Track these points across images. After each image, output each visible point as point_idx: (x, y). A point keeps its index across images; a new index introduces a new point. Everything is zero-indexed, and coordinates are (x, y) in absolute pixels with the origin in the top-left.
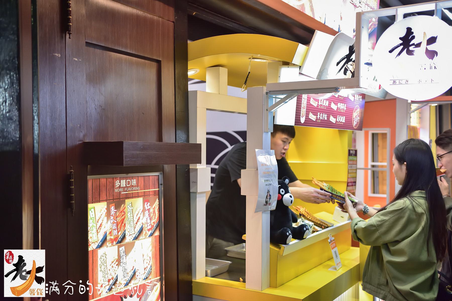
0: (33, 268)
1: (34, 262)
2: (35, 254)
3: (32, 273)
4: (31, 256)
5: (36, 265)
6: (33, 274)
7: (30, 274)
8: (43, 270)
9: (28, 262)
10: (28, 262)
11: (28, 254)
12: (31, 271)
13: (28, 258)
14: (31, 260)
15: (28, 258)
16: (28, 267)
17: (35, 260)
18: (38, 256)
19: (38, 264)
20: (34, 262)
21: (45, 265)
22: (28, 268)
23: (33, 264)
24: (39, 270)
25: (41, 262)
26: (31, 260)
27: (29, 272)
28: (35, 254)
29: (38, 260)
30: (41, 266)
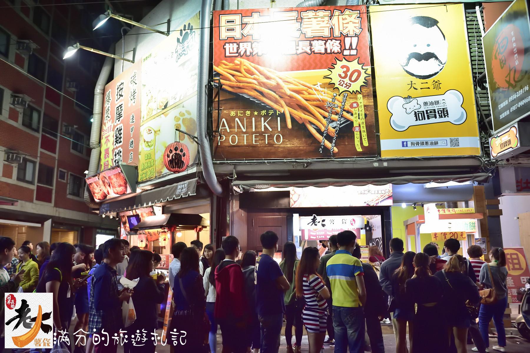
0: (39, 314)
1: (40, 307)
2: (41, 297)
3: (37, 320)
4: (37, 300)
5: (42, 311)
6: (39, 321)
7: (35, 321)
8: (51, 316)
9: (32, 308)
10: (32, 308)
11: (32, 297)
12: (36, 317)
13: (32, 302)
14: (37, 305)
15: (32, 302)
16: (32, 313)
17: (41, 305)
18: (45, 300)
19: (45, 310)
20: (40, 307)
21: (52, 311)
22: (33, 314)
23: (38, 309)
24: (46, 316)
25: (48, 308)
26: (37, 305)
27: (34, 320)
28: (41, 297)
29: (45, 305)
30: (48, 312)
